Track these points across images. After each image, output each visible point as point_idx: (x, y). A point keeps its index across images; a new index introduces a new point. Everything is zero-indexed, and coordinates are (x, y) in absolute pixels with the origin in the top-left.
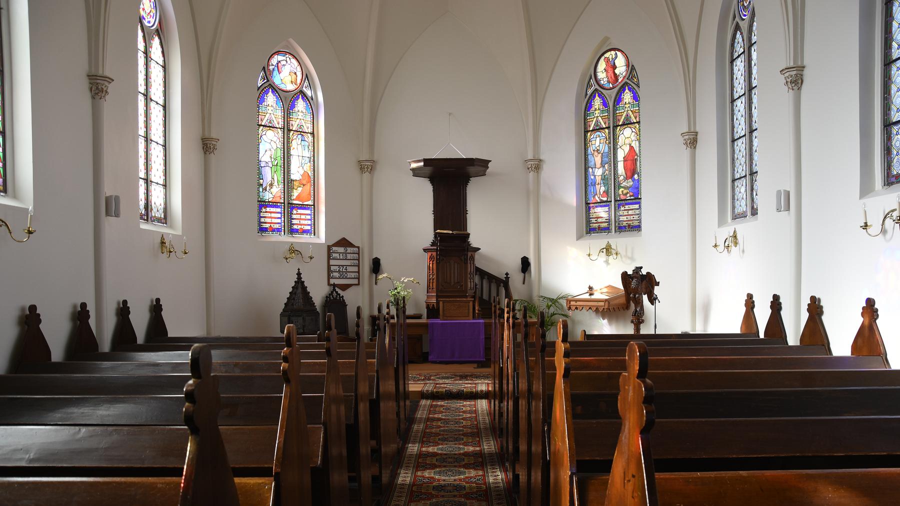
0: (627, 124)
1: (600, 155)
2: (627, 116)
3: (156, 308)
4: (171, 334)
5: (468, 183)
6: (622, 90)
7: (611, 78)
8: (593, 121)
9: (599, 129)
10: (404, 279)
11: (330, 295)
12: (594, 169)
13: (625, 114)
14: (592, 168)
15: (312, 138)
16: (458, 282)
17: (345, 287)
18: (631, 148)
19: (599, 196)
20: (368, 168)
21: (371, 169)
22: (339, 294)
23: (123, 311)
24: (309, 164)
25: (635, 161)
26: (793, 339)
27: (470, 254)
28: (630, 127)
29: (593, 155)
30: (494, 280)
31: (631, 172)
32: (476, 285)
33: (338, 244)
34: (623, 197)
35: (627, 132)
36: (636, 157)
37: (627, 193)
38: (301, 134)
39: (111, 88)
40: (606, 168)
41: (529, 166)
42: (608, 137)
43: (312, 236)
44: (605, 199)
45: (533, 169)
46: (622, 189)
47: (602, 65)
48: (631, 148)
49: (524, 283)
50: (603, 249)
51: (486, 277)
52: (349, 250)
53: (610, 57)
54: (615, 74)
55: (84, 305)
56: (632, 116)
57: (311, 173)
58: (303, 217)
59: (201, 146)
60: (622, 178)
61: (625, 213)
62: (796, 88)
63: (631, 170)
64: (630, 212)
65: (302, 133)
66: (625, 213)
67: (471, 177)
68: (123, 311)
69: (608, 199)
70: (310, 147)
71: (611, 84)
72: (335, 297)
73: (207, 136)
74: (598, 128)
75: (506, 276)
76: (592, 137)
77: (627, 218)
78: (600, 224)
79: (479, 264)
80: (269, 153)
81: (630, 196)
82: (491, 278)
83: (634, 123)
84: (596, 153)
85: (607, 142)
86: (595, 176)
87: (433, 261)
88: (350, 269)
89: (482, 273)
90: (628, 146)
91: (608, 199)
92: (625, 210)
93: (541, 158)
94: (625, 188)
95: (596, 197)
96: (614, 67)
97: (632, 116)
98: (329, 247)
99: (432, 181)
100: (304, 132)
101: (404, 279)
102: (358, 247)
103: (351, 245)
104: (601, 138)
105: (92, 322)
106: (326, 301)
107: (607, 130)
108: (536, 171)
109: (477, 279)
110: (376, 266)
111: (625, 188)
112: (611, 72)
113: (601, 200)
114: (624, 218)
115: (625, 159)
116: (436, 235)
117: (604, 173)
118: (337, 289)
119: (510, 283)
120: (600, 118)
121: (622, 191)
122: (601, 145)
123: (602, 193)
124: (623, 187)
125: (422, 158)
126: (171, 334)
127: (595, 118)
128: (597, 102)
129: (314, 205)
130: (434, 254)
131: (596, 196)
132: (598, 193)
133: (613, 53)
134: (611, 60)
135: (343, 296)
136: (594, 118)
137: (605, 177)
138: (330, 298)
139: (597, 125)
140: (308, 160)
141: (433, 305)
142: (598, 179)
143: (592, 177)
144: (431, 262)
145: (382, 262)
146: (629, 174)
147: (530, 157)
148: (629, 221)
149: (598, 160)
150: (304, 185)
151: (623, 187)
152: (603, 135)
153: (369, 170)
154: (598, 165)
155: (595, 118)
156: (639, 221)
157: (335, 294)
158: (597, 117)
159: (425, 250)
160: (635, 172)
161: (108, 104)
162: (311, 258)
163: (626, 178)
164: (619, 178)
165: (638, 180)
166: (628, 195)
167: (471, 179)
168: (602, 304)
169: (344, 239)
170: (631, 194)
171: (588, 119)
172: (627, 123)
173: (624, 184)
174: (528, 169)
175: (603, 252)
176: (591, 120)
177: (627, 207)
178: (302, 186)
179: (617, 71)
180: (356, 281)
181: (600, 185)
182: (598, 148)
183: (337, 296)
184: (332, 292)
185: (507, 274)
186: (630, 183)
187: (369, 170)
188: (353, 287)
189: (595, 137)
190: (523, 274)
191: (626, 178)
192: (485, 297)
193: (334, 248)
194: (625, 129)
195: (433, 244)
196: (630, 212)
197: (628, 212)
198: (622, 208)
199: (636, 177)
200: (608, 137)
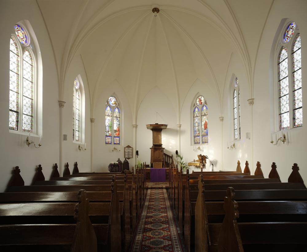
3: (76, 165)
4: (80, 172)
6: (203, 106)
17: (129, 158)
18: (206, 121)
23: (67, 166)
26: (252, 173)
33: (127, 147)
35: (205, 117)
39: (65, 105)
47: (198, 100)
48: (206, 121)
52: (130, 148)
54: (201, 102)
55: (56, 164)
59: (90, 121)
61: (204, 139)
62: (252, 105)
64: (206, 139)
66: (204, 139)
68: (67, 166)
73: (92, 118)
79: (164, 152)
80: (108, 123)
82: (168, 156)
88: (130, 152)
89: (165, 155)
94: (204, 132)
96: (201, 100)
103: (131, 147)
105: (58, 169)
109: (164, 156)
110: (137, 152)
112: (200, 102)
114: (204, 140)
115: (204, 125)
126: (80, 172)
128: (196, 110)
130: (153, 149)
133: (201, 97)
142: (197, 130)
149: (197, 125)
154: (197, 126)
159: (150, 148)
161: (64, 109)
172: (205, 115)
173: (204, 131)
177: (205, 137)
179: (202, 101)
180: (132, 157)
185: (172, 155)
186: (205, 131)
192: (166, 161)
193: (126, 148)
195: (152, 147)
196: (206, 139)
199: (207, 129)
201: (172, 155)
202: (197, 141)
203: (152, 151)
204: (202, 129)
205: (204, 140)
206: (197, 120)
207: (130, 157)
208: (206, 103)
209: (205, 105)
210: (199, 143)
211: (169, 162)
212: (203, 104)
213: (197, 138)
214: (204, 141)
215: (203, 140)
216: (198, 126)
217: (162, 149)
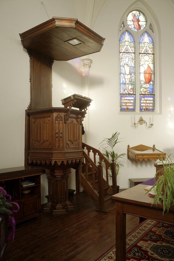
1: (129, 67)
7: (136, 26)
8: (124, 47)
9: (128, 53)
12: (124, 75)
13: (145, 48)
14: (123, 74)
18: (149, 67)
19: (127, 90)
25: (151, 75)
28: (148, 56)
29: (124, 66)
35: (146, 58)
36: (152, 72)
37: (146, 91)
40: (133, 75)
42: (134, 58)
44: (132, 93)
46: (143, 89)
53: (136, 14)
54: (139, 25)
56: (149, 50)
60: (143, 82)
61: (145, 102)
63: (148, 79)
64: (148, 102)
66: (145, 102)
69: (133, 93)
71: (136, 29)
74: (127, 52)
76: (123, 56)
78: (128, 107)
81: (148, 93)
84: (126, 66)
85: (133, 61)
86: (125, 79)
90: (147, 65)
91: (133, 93)
94: (145, 88)
95: (126, 91)
97: (149, 50)
104: (129, 58)
111: (145, 88)
114: (144, 105)
117: (131, 78)
120: (129, 46)
121: (143, 90)
122: (129, 62)
123: (129, 89)
124: (143, 87)
127: (126, 46)
132: (127, 89)
134: (136, 16)
136: (125, 46)
137: (132, 80)
139: (127, 50)
142: (128, 82)
143: (124, 79)
146: (147, 81)
148: (146, 106)
149: (127, 70)
151: (143, 87)
152: (131, 56)
155: (126, 46)
158: (127, 45)
160: (151, 80)
163: (146, 83)
165: (153, 85)
166: (147, 92)
170: (149, 92)
171: (120, 46)
173: (144, 86)
177: (146, 99)
179: (140, 23)
182: (127, 63)
186: (148, 86)
189: (125, 56)
191: (146, 83)
194: (145, 56)
196: (148, 102)
198: (143, 99)
199: (151, 83)
200: (134, 58)
202: (128, 104)
204: (140, 81)
205: (144, 105)
206: (127, 60)
208: (151, 27)
209: (150, 31)
210: (134, 110)
212: (142, 29)
213: (125, 98)
214: (144, 108)
215: (142, 105)
216: (130, 74)
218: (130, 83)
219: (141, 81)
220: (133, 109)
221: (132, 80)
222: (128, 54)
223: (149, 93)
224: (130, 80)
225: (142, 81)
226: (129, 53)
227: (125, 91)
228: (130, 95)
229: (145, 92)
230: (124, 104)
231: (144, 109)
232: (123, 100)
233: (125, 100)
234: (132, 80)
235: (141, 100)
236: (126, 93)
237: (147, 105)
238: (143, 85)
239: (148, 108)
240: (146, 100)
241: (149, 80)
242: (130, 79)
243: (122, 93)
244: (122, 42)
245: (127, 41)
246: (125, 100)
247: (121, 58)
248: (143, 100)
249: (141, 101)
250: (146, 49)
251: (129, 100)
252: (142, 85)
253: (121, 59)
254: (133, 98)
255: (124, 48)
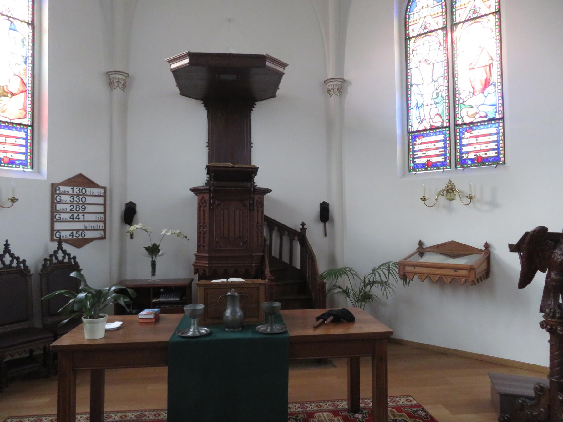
0: (477, 18)
1: (431, 66)
2: (475, 7)
5: (255, 106)
9: (428, 32)
10: (167, 231)
11: (51, 256)
14: (417, 85)
15: (31, 31)
16: (240, 237)
17: (80, 242)
19: (428, 120)
20: (119, 82)
21: (124, 85)
22: (69, 255)
24: (24, 66)
27: (256, 197)
30: (286, 233)
31: (482, 84)
32: (265, 241)
33: (69, 182)
34: (467, 120)
38: (8, 19)
41: (331, 88)
43: (29, 169)
45: (335, 90)
49: (326, 235)
50: (443, 191)
51: (276, 228)
57: (28, 81)
58: (9, 140)
61: (473, 140)
63: (481, 81)
64: (480, 140)
65: (11, 19)
66: (473, 140)
67: (257, 101)
70: (26, 43)
72: (60, 258)
74: (426, 31)
75: (301, 227)
76: (417, 44)
77: (475, 148)
79: (268, 211)
81: (481, 117)
82: (283, 229)
83: (486, 15)
85: (442, 48)
87: (205, 207)
88: (67, 216)
89: (272, 224)
92: (471, 137)
93: (345, 78)
98: (54, 188)
99: (207, 105)
100: (14, 18)
101: (167, 231)
102: (104, 188)
103: (93, 185)
106: (44, 266)
107: (440, 32)
108: (338, 94)
113: (431, 126)
116: (209, 170)
118: (65, 246)
119: (308, 235)
125: (185, 52)
127: (422, 19)
129: (32, 126)
130: (206, 197)
131: (424, 122)
132: (427, 118)
135: (74, 258)
138: (51, 260)
140: (23, 60)
141: (204, 270)
142: (428, 100)
144: (202, 208)
145: (138, 209)
147: (331, 75)
150: (13, 95)
153: (120, 85)
155: (422, 19)
156: (496, 151)
157: (60, 255)
159: (195, 191)
160: (489, 82)
162: (13, 200)
164: (460, 94)
166: (478, 116)
167: (256, 103)
168: (465, 273)
169: (81, 176)
170: (483, 114)
174: (330, 91)
175: (443, 195)
176: (415, 22)
177: (475, 133)
178: (9, 95)
181: (431, 105)
182: (427, 58)
183: (64, 258)
184: (56, 252)
185: (303, 224)
187: (120, 85)
188: (94, 242)
190: (321, 225)
192: (275, 253)
193: (63, 188)
196: (480, 140)
197: (477, 140)
198: (467, 135)
201: (303, 224)
202: (429, 153)
203: (201, 204)
207: (89, 235)
211: (286, 259)
213: (424, 140)
214: (472, 156)
217: (256, 197)
218: (433, 102)
219: (461, 92)
220: (442, 162)
221: (437, 93)
222: (429, 35)
223: (486, 117)
224: (435, 96)
225: (464, 90)
226: (430, 34)
227: (422, 121)
228: (434, 131)
229: (473, 116)
230: (420, 154)
231: (472, 160)
232: (419, 144)
233: (422, 143)
234: (440, 95)
235: (463, 138)
236: (425, 127)
237: (479, 147)
238: (465, 100)
239: (484, 156)
240: (477, 137)
241: (484, 83)
242: (433, 93)
243: (415, 130)
244: (413, 14)
245: (425, 6)
246: (422, 143)
247: (413, 51)
248: (467, 138)
249: (463, 140)
250: (475, 7)
251: (431, 142)
252: (464, 102)
253: (412, 53)
254: (441, 137)
255: (419, 25)
